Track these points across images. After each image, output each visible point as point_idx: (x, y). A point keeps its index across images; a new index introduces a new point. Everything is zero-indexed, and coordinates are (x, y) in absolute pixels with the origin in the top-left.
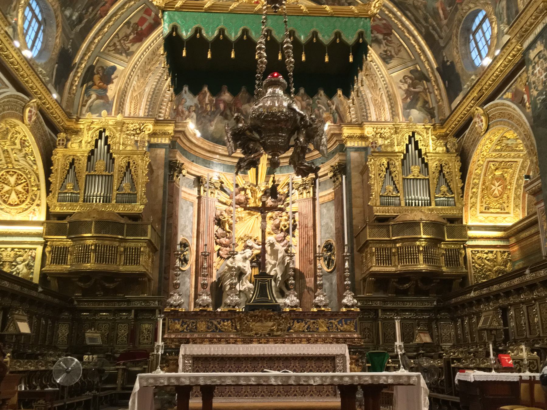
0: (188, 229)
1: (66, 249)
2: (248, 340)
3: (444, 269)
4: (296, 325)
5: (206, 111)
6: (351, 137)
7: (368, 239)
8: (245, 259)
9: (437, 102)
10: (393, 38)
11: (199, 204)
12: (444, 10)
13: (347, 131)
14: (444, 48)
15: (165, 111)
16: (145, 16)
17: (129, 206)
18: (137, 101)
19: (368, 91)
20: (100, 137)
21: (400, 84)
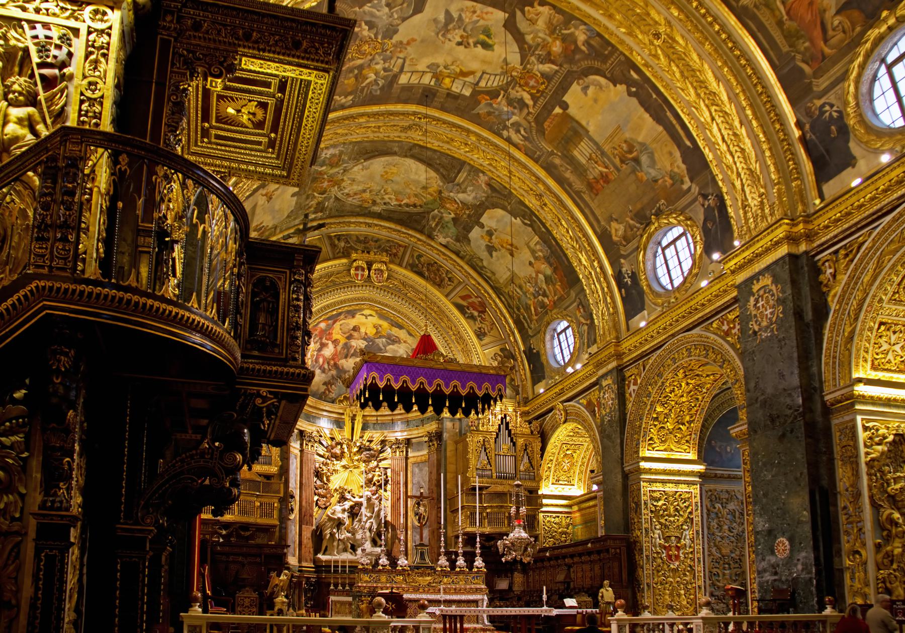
9: (522, 381)
10: (485, 316)
12: (536, 310)
14: (532, 337)
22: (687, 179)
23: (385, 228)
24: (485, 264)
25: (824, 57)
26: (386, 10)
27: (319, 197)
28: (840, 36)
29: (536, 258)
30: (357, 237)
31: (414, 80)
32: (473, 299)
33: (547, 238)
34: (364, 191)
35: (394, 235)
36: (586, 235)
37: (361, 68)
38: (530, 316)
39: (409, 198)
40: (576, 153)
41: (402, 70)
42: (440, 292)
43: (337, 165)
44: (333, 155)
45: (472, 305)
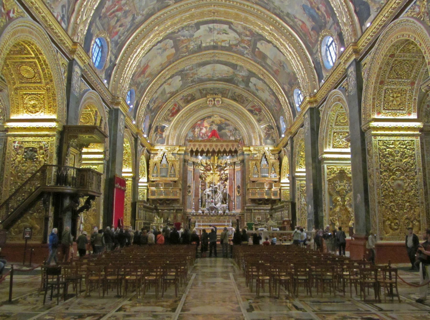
0: (190, 181)
1: (155, 191)
2: (210, 222)
3: (273, 197)
4: (221, 218)
5: (195, 137)
6: (246, 150)
7: (248, 187)
8: (210, 191)
10: (262, 114)
13: (244, 149)
15: (182, 142)
18: (173, 140)
20: (164, 155)
23: (221, 84)
24: (258, 94)
26: (187, 32)
27: (192, 79)
30: (210, 88)
31: (208, 44)
32: (256, 107)
34: (207, 74)
35: (224, 86)
36: (279, 88)
37: (186, 46)
40: (267, 62)
41: (201, 43)
42: (243, 106)
43: (192, 69)
45: (256, 109)
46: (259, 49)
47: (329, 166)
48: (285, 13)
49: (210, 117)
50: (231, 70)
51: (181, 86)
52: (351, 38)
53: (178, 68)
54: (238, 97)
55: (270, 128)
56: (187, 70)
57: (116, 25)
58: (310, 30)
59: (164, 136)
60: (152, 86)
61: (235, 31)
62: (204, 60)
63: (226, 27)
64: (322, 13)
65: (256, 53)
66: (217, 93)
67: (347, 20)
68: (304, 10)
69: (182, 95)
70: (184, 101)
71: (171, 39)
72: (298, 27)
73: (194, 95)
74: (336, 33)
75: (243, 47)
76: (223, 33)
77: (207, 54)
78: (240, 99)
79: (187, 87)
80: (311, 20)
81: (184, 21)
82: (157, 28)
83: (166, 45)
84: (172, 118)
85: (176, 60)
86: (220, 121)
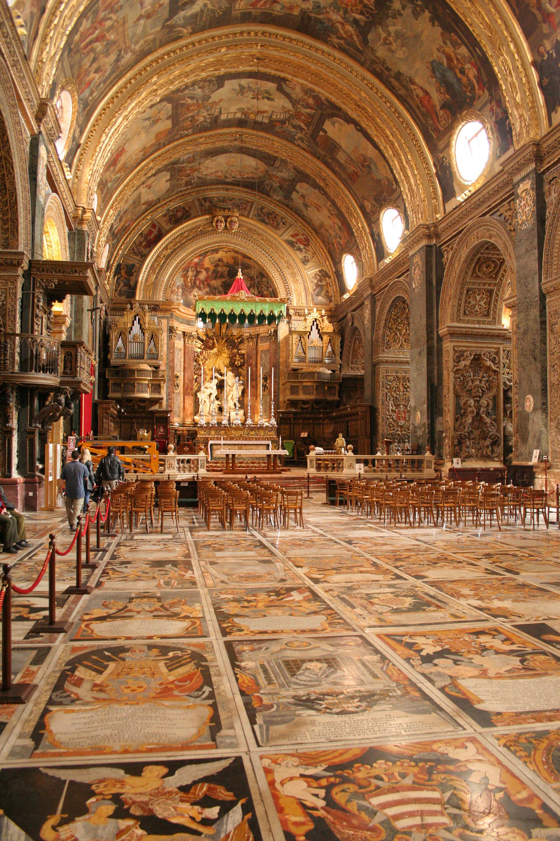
0: (178, 366)
2: (232, 439)
9: (334, 293)
11: (184, 349)
16: (153, 230)
17: (154, 361)
19: (292, 285)
21: (313, 280)
22: (394, 183)
24: (305, 213)
25: (440, 131)
26: (200, 90)
27: (187, 179)
28: (444, 122)
29: (331, 214)
31: (230, 116)
32: (301, 237)
33: (334, 203)
34: (217, 172)
36: (353, 206)
37: (193, 117)
38: (335, 249)
39: (248, 174)
40: (338, 157)
41: (220, 113)
42: (276, 234)
43: (193, 161)
44: (190, 158)
46: (325, 132)
47: (457, 346)
48: (392, 73)
49: (216, 251)
50: (262, 166)
51: (167, 192)
52: (528, 132)
53: (171, 158)
54: (268, 218)
55: (324, 275)
56: (183, 162)
57: (91, 69)
58: (438, 107)
59: (132, 283)
60: (124, 188)
61: (287, 96)
62: (218, 144)
63: (271, 86)
64: (469, 79)
65: (318, 140)
66: (231, 207)
67: (522, 99)
68: (433, 71)
69: (166, 207)
70: (170, 219)
71: (169, 103)
72: (414, 99)
73: (187, 209)
74: (494, 119)
75: (294, 127)
76: (263, 98)
77: (225, 134)
78: (271, 222)
79: (177, 193)
80: (442, 90)
81: (203, 70)
82: (155, 79)
83: (159, 113)
84: (149, 249)
85: (169, 143)
86: (234, 258)
